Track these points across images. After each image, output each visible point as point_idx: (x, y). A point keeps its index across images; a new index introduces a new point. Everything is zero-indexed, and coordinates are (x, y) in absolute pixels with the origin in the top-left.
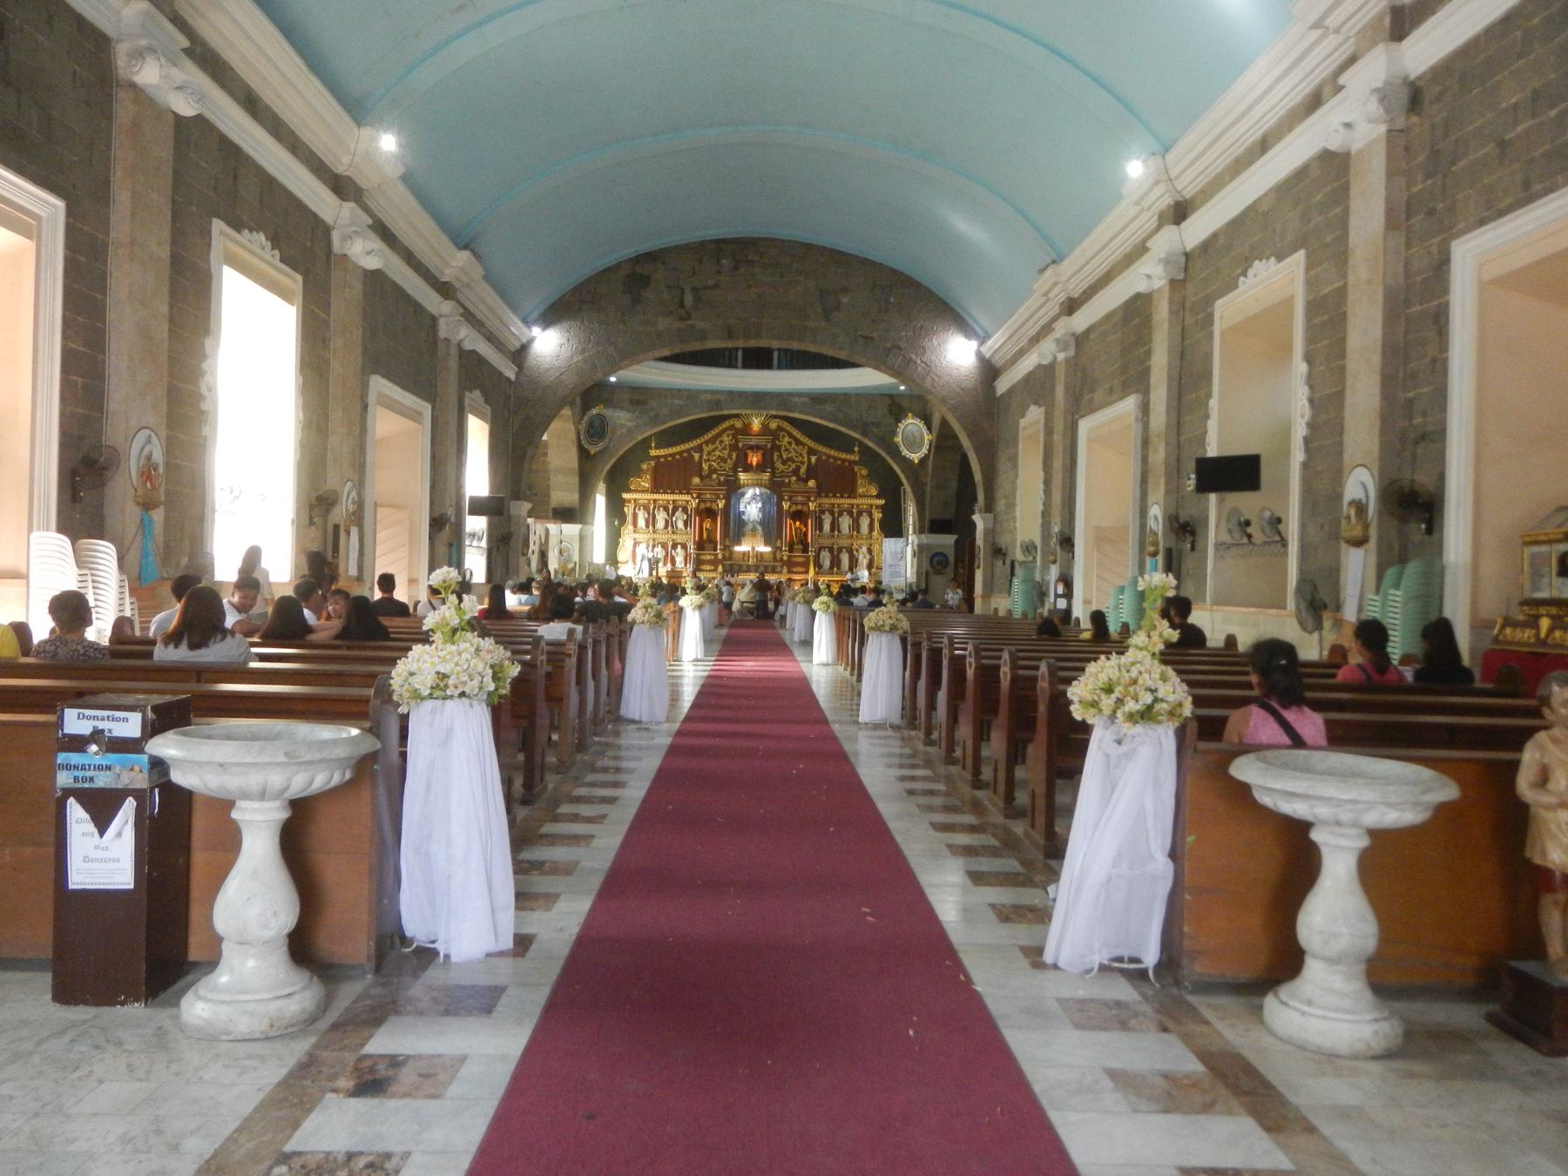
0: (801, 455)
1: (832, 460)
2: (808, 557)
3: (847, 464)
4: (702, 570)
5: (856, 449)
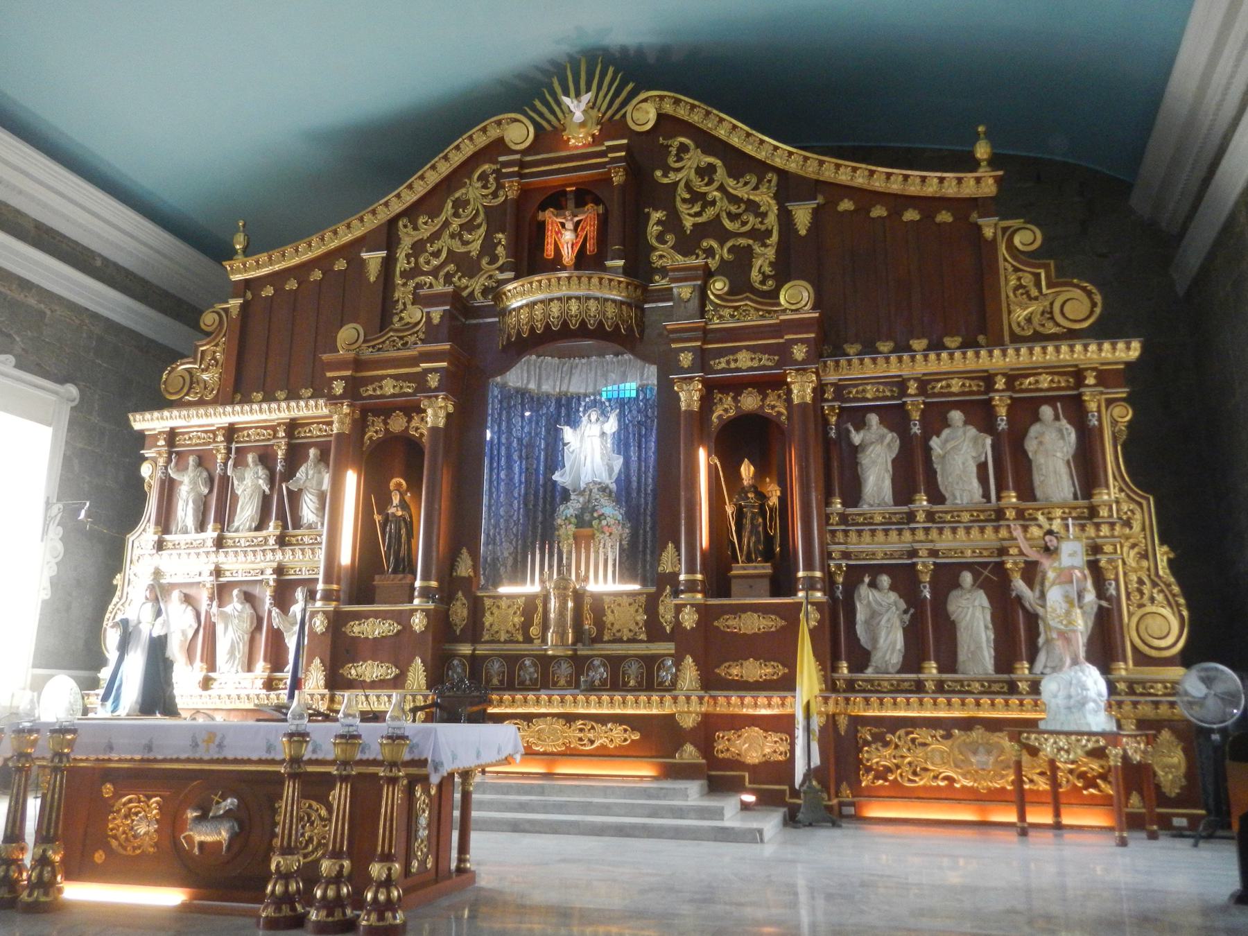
0: (752, 206)
2: (791, 615)
4: (350, 684)
5: (982, 151)
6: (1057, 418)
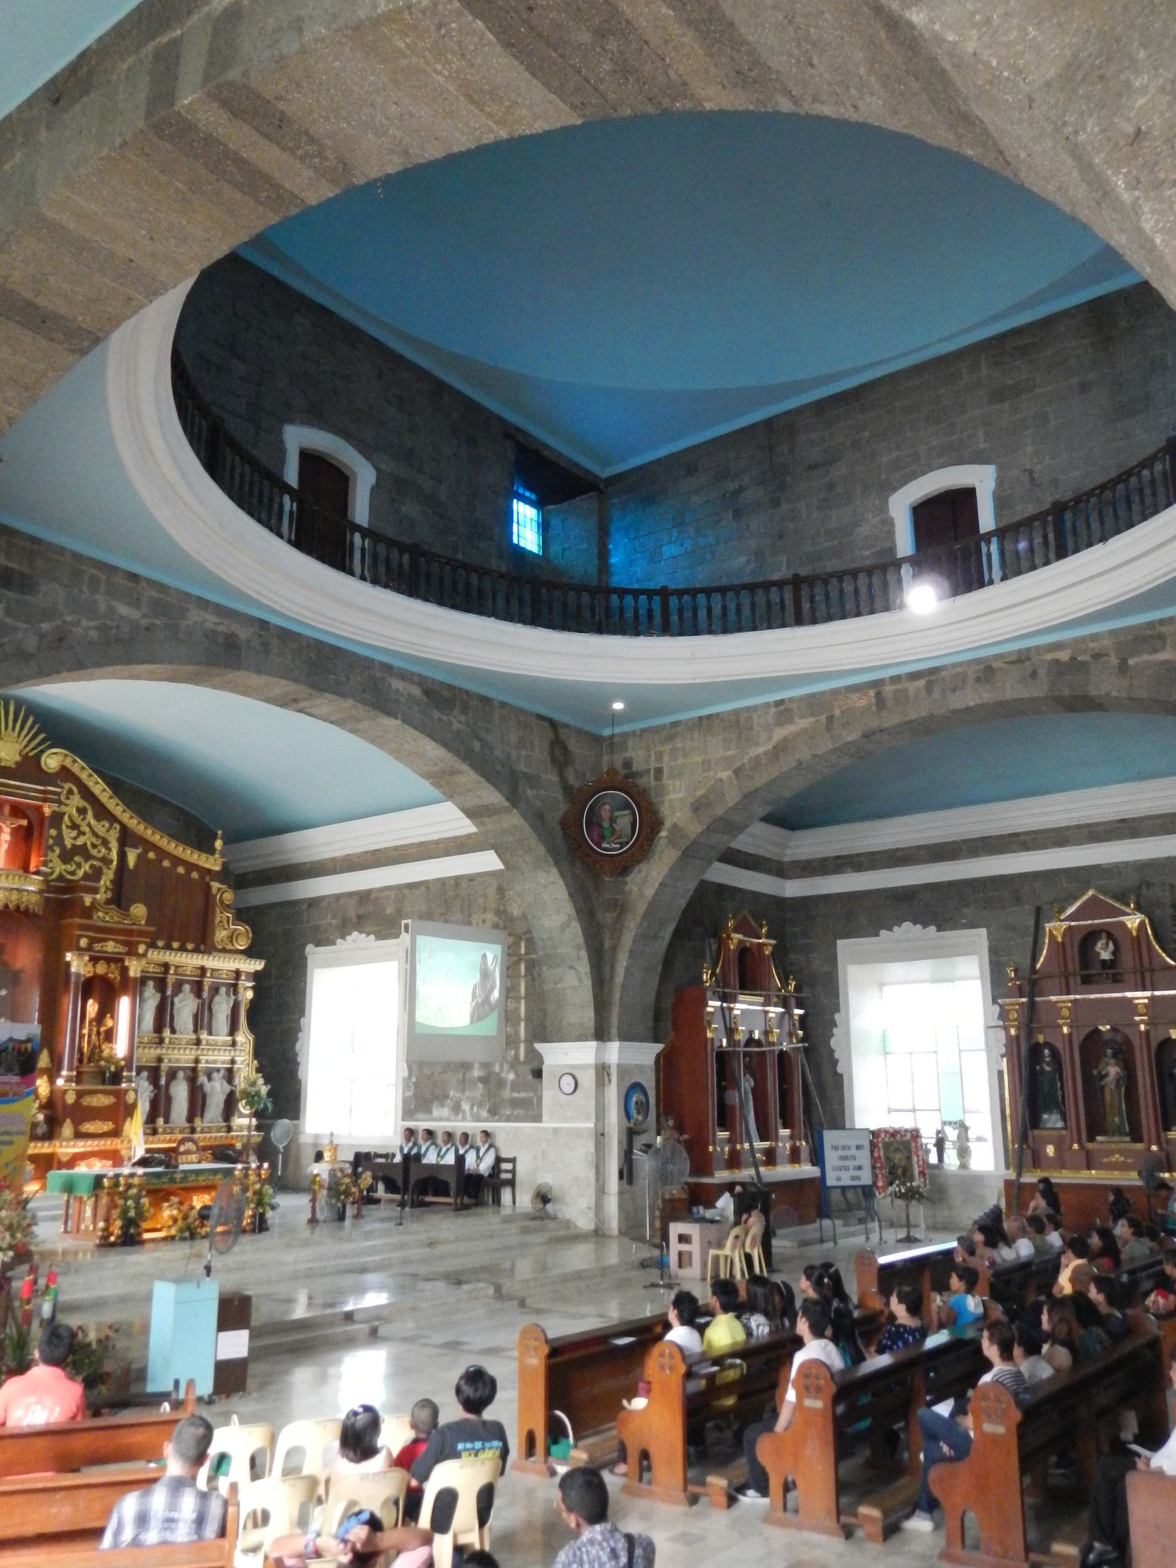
0: (105, 843)
1: (166, 863)
3: (195, 875)
5: (218, 844)
6: (228, 994)
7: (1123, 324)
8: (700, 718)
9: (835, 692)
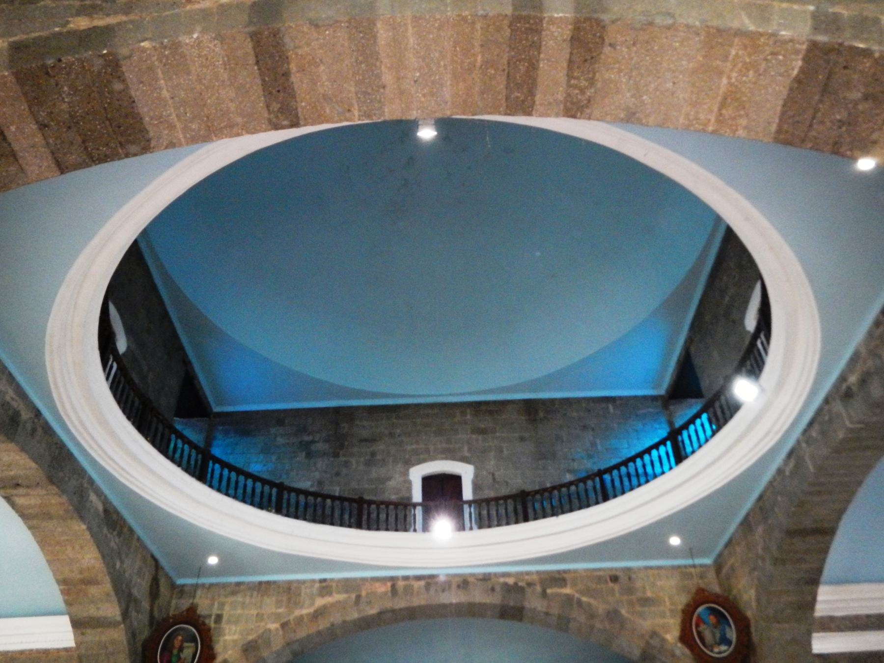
7: (541, 414)
8: (260, 583)
9: (364, 580)
